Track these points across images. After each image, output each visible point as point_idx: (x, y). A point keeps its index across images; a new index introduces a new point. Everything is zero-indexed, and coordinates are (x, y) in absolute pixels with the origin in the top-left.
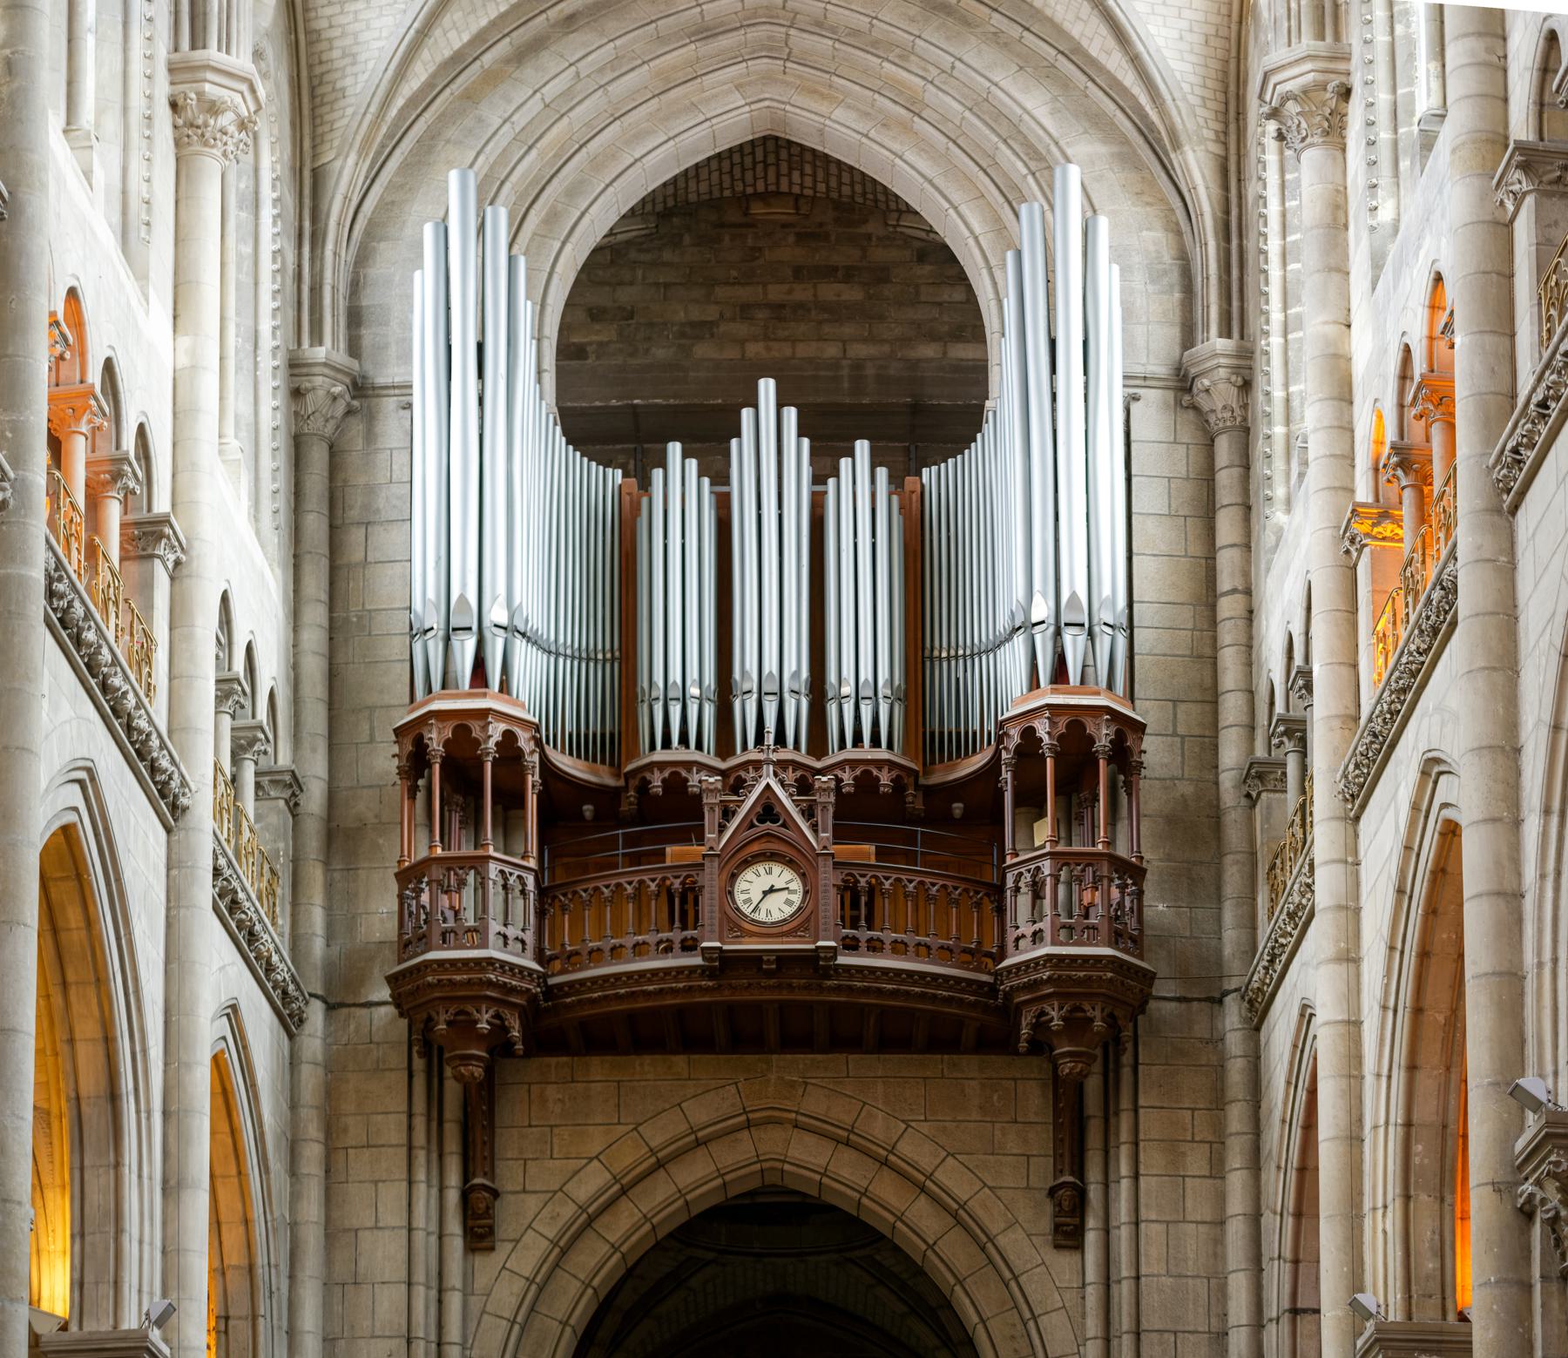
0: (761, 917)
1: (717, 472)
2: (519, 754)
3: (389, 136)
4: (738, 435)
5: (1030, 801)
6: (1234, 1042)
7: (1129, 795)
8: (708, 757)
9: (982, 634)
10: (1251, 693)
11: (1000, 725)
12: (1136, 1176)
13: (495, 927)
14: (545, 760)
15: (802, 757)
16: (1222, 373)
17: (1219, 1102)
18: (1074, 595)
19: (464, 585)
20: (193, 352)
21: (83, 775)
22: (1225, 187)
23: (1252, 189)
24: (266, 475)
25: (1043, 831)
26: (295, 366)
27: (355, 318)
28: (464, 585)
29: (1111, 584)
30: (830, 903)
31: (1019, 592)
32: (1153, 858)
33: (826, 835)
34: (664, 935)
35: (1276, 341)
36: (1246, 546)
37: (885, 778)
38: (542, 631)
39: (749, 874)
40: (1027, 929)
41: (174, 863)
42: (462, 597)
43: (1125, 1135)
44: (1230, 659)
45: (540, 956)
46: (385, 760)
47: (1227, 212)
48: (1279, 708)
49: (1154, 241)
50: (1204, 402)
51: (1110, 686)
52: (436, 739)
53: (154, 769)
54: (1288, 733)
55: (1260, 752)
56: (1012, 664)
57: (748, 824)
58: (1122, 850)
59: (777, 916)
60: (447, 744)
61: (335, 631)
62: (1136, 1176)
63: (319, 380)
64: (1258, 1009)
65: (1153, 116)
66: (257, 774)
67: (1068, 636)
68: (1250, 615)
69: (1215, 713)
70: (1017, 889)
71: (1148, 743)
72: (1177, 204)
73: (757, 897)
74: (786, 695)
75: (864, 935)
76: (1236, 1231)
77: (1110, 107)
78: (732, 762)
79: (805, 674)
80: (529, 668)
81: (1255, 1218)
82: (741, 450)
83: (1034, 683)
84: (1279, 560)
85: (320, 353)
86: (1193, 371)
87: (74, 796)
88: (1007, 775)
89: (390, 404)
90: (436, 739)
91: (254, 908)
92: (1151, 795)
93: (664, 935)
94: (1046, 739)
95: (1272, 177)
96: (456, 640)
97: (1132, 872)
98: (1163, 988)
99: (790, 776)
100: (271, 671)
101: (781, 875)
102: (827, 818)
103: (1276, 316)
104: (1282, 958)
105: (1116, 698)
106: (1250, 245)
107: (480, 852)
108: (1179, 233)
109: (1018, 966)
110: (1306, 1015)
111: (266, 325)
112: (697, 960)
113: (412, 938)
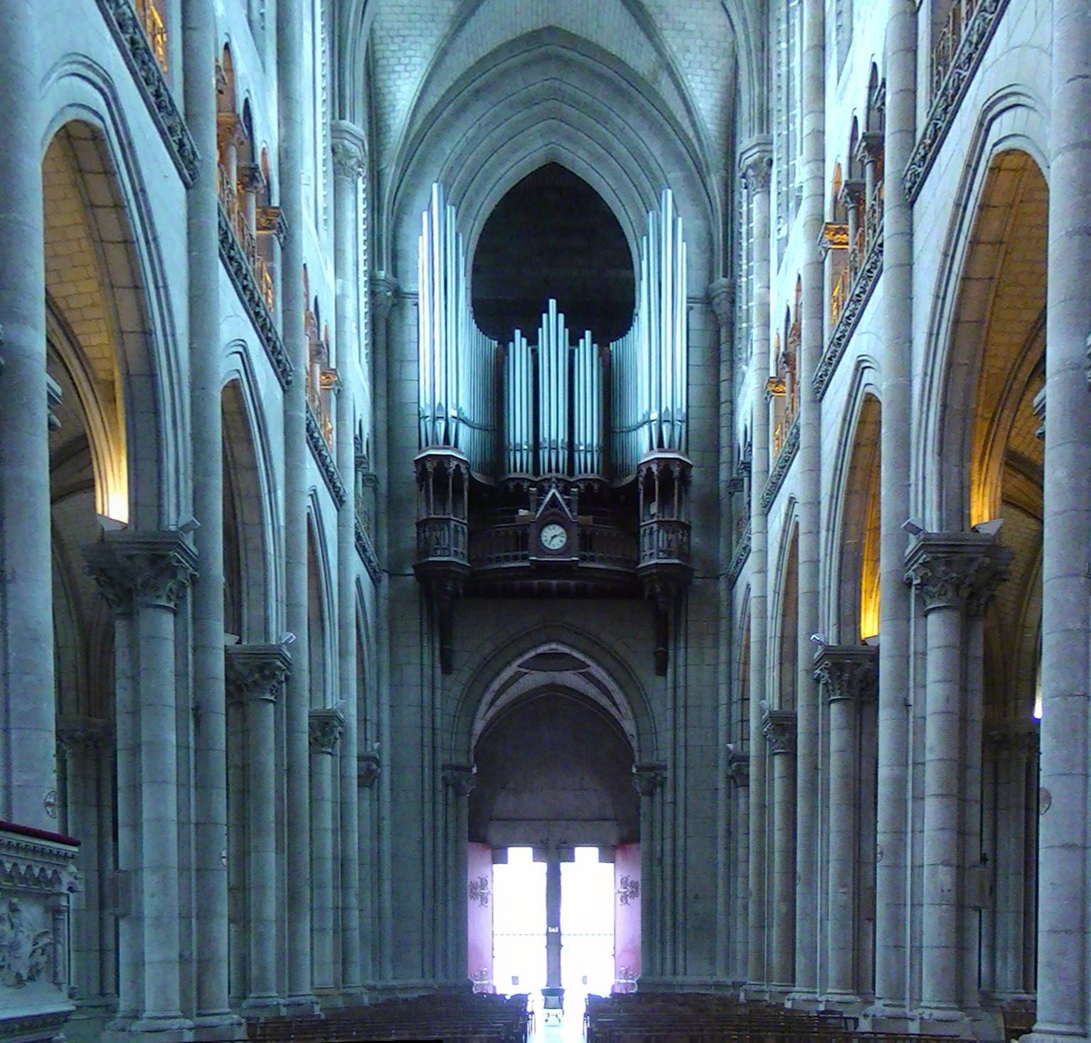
0: (551, 547)
1: (533, 341)
6: (723, 594)
9: (631, 422)
10: (731, 447)
12: (686, 648)
13: (453, 549)
15: (565, 477)
17: (717, 618)
19: (440, 398)
25: (654, 509)
26: (373, 281)
27: (395, 256)
29: (681, 403)
30: (576, 541)
31: (646, 407)
32: (695, 521)
33: (575, 514)
34: (516, 553)
36: (731, 380)
37: (596, 487)
39: (546, 530)
40: (648, 553)
43: (682, 632)
44: (724, 433)
48: (742, 458)
50: (718, 311)
52: (430, 466)
55: (735, 475)
58: (683, 520)
59: (557, 547)
62: (686, 648)
64: (732, 582)
67: (664, 427)
68: (732, 413)
69: (718, 458)
71: (694, 472)
73: (549, 539)
74: (560, 450)
76: (723, 668)
79: (566, 440)
81: (730, 662)
82: (542, 333)
83: (651, 448)
86: (713, 294)
89: (409, 302)
90: (430, 466)
91: (364, 535)
92: (694, 492)
93: (516, 553)
94: (656, 473)
96: (437, 423)
97: (686, 527)
98: (696, 574)
99: (561, 485)
101: (558, 530)
102: (575, 506)
104: (741, 563)
107: (447, 517)
110: (748, 588)
113: (424, 549)
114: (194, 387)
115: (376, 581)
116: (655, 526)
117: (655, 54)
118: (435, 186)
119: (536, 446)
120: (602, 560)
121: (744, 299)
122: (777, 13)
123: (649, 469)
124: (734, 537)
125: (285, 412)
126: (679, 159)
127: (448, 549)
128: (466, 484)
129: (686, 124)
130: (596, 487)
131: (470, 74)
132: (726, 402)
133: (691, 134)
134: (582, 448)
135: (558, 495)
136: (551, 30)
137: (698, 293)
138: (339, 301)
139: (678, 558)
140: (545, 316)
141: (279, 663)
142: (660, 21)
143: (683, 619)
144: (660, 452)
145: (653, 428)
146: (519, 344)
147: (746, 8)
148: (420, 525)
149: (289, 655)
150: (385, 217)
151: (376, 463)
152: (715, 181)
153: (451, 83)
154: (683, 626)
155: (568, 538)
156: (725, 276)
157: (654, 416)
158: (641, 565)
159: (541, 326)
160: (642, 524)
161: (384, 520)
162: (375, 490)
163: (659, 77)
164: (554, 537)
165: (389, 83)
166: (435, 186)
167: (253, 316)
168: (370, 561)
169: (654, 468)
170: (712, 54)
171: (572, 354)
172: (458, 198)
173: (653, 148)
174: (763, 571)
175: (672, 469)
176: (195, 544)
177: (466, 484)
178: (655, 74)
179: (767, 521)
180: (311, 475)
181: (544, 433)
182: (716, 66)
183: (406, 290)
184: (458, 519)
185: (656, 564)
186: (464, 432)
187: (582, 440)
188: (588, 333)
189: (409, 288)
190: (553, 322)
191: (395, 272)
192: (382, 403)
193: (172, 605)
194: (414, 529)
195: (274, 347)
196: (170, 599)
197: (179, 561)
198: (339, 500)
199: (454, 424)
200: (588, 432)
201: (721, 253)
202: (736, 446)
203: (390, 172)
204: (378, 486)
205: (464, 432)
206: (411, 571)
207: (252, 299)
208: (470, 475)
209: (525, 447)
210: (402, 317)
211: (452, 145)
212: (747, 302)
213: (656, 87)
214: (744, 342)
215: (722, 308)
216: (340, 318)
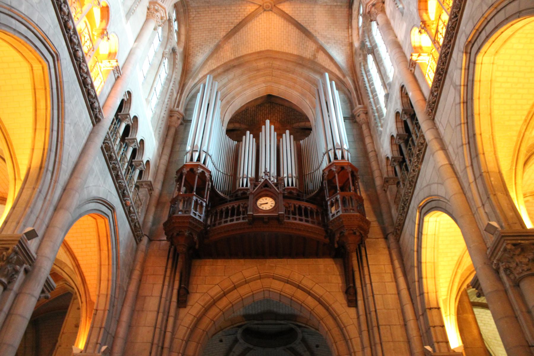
2: (205, 177)
18: (337, 143)
28: (198, 142)
67: (337, 151)
143: (365, 264)
153: (223, 63)
154: (366, 269)
155: (276, 203)
156: (360, 104)
157: (330, 146)
159: (261, 131)
161: (153, 209)
163: (317, 56)
171: (278, 141)
178: (314, 56)
204: (153, 192)
213: (316, 61)
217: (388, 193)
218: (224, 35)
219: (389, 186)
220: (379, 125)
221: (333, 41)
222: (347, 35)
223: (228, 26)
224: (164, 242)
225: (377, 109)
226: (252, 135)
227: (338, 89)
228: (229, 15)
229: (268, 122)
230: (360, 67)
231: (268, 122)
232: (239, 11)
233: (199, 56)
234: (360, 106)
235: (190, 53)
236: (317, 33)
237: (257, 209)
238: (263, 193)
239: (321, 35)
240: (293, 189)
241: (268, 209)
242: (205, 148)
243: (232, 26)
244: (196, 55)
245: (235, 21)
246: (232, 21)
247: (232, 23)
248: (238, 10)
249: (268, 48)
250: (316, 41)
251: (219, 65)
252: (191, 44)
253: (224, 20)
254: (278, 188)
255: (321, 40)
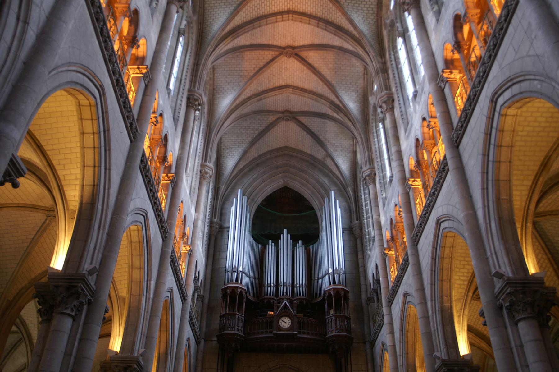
2: (243, 295)
3: (229, 183)
4: (281, 239)
5: (330, 307)
7: (347, 304)
8: (274, 297)
10: (366, 285)
11: (325, 291)
13: (236, 327)
14: (247, 297)
16: (357, 227)
18: (336, 268)
20: (198, 216)
21: (170, 290)
22: (355, 194)
23: (359, 194)
24: (205, 241)
25: (332, 312)
27: (221, 214)
31: (327, 267)
35: (365, 221)
36: (363, 258)
38: (247, 273)
40: (331, 330)
41: (183, 310)
42: (235, 266)
44: (362, 279)
45: (244, 333)
46: (219, 295)
47: (356, 198)
48: (372, 287)
49: (344, 203)
51: (343, 284)
52: (228, 291)
53: (182, 291)
54: (374, 292)
55: (369, 296)
56: (326, 280)
57: (282, 310)
58: (346, 314)
60: (231, 292)
61: (213, 270)
63: (215, 225)
65: (343, 182)
66: (197, 295)
70: (328, 322)
71: (350, 295)
72: (348, 198)
75: (302, 331)
77: (337, 181)
78: (278, 298)
80: (245, 279)
84: (370, 260)
85: (216, 220)
87: (168, 294)
88: (326, 301)
89: (226, 230)
90: (228, 291)
92: (351, 305)
95: (362, 192)
100: (201, 276)
102: (295, 309)
103: (365, 216)
105: (344, 286)
106: (360, 204)
107: (235, 313)
108: (349, 203)
109: (329, 337)
111: (208, 214)
112: (272, 335)
113: (222, 327)
114: (113, 214)
115: (198, 343)
116: (334, 318)
117: (324, 152)
118: (239, 190)
119: (277, 285)
120: (308, 334)
121: (366, 227)
122: (372, 131)
123: (330, 293)
124: (371, 323)
125: (162, 249)
126: (335, 183)
127: (234, 327)
128: (245, 300)
129: (337, 173)
130: (304, 302)
131: (255, 159)
132: (362, 266)
133: (339, 176)
134: (298, 285)
135: (287, 303)
136: (286, 148)
137: (346, 227)
138: (195, 222)
139: (345, 332)
140: (282, 235)
141: (136, 366)
142: (326, 142)
144: (334, 285)
145: (330, 276)
146: (271, 249)
147: (360, 131)
148: (222, 317)
149: (142, 363)
150: (219, 201)
151: (204, 290)
152: (350, 190)
157: (331, 271)
158: (327, 336)
160: (327, 317)
161: (205, 315)
162: (202, 302)
164: (285, 323)
165: (225, 161)
166: (239, 190)
167: (153, 204)
168: (196, 332)
169: (332, 293)
170: (346, 152)
172: (249, 195)
173: (326, 181)
174: (392, 332)
175: (340, 292)
176: (95, 284)
177: (245, 300)
178: (324, 158)
179: (391, 309)
180: (170, 281)
181: (281, 280)
182: (347, 156)
183: (225, 226)
184: (240, 315)
185: (335, 335)
186: (245, 279)
187: (298, 282)
188: (300, 242)
189: (226, 225)
190: (285, 238)
191: (221, 220)
192: (210, 267)
193: (73, 314)
194: (219, 319)
195: (161, 219)
196: (72, 311)
197: (82, 290)
198: (184, 298)
199: (241, 274)
200: (301, 279)
201: (355, 213)
202: (369, 284)
203: (223, 188)
205: (245, 279)
206: (216, 339)
207: (154, 195)
208: (246, 296)
209: (272, 285)
210: (222, 236)
211: (247, 181)
212: (368, 229)
213: (325, 162)
214: (368, 243)
215: (358, 232)
216: (195, 227)
217: (369, 307)
218: (250, 140)
219: (370, 304)
220: (369, 248)
221: (341, 149)
222: (352, 143)
223: (253, 132)
224: (215, 342)
225: (368, 231)
226: (273, 244)
227: (340, 207)
228: (254, 122)
229: (285, 231)
230: (360, 182)
231: (285, 231)
232: (263, 120)
233: (229, 158)
234: (356, 222)
235: (221, 154)
236: (327, 142)
237: (279, 328)
238: (283, 314)
239: (331, 143)
240: (303, 299)
241: (287, 327)
242: (241, 269)
243: (257, 133)
244: (227, 158)
245: (260, 128)
246: (257, 128)
247: (257, 130)
248: (262, 119)
249: (286, 145)
250: (326, 150)
251: (245, 164)
252: (222, 145)
253: (250, 127)
254: (293, 311)
255: (330, 148)
